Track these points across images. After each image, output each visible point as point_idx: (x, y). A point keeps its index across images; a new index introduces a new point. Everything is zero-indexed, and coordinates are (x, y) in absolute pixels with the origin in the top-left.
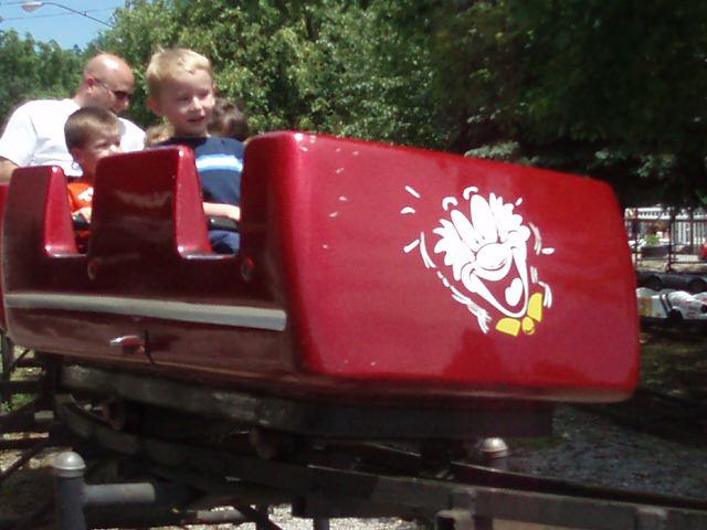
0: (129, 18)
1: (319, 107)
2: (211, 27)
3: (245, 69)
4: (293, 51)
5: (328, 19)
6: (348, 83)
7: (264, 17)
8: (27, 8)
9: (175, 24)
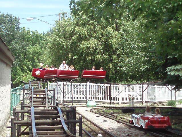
2: (86, 27)
3: (96, 40)
4: (111, 34)
6: (129, 45)
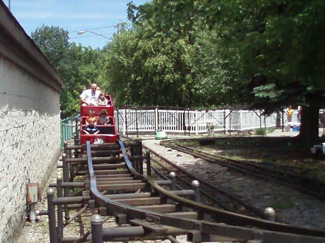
0: (118, 37)
1: (194, 71)
2: (151, 40)
3: (165, 56)
4: (184, 49)
5: (198, 36)
6: (206, 62)
7: (172, 35)
8: (80, 34)
9: (137, 39)
